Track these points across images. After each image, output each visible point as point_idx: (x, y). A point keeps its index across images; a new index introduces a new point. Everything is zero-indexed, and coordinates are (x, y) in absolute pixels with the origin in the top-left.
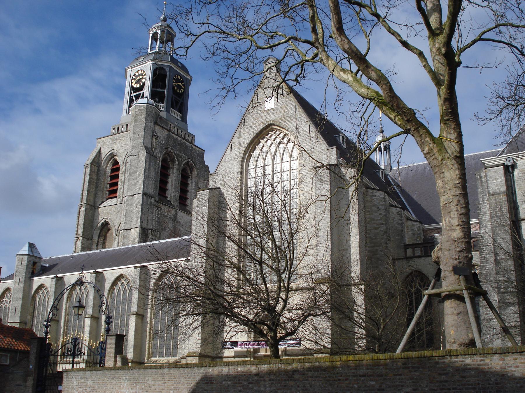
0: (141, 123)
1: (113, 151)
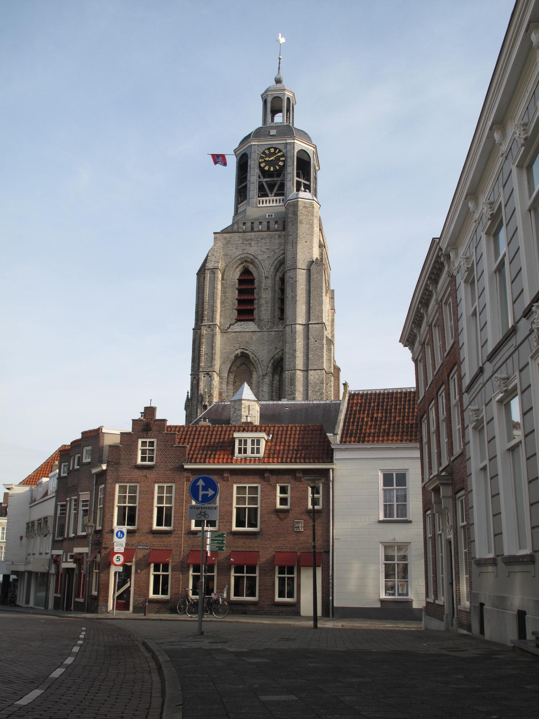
0: (308, 226)
1: (246, 255)
